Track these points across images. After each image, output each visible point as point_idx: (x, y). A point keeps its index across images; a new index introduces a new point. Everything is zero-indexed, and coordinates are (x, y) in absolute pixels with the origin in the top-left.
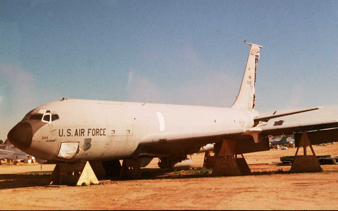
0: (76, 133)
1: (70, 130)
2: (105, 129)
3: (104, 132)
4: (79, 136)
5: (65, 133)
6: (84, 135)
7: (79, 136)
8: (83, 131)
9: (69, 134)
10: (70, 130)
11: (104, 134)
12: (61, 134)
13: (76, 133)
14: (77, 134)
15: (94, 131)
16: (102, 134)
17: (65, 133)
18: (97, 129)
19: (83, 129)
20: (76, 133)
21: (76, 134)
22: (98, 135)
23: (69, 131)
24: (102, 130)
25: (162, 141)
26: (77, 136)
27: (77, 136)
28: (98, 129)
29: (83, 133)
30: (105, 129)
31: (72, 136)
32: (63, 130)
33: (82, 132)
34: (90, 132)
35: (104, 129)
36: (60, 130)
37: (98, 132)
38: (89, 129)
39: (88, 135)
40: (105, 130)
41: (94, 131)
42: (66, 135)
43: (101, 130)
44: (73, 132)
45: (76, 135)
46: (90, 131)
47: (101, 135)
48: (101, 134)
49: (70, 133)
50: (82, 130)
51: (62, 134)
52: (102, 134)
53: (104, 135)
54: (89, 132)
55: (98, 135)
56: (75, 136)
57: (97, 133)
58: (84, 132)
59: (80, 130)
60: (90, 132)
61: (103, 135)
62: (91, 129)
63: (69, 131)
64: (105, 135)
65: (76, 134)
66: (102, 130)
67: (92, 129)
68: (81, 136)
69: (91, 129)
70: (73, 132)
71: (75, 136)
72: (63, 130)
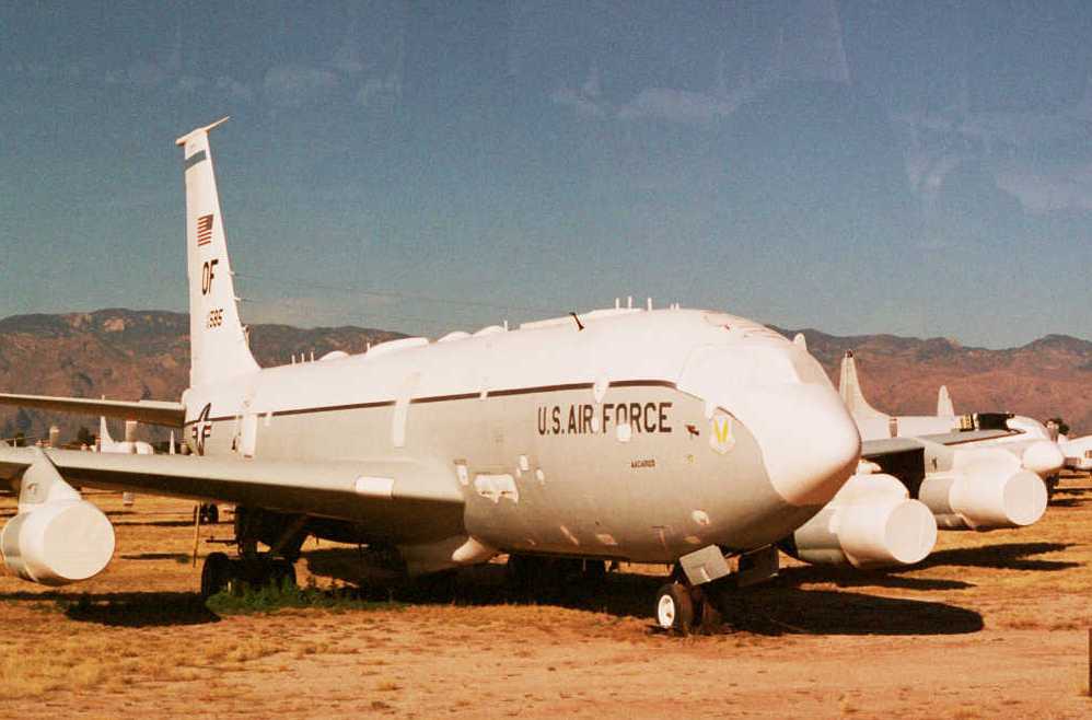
2: (669, 405)
3: (663, 417)
5: (551, 425)
11: (665, 424)
16: (654, 426)
17: (551, 425)
22: (639, 430)
26: (575, 432)
28: (637, 405)
29: (588, 419)
30: (669, 405)
35: (663, 405)
39: (605, 431)
40: (664, 409)
42: (552, 432)
43: (650, 410)
45: (572, 430)
46: (609, 412)
48: (650, 425)
50: (587, 407)
52: (654, 426)
54: (606, 418)
55: (639, 430)
57: (634, 422)
59: (580, 407)
61: (657, 428)
62: (611, 406)
64: (669, 430)
65: (572, 426)
67: (616, 406)
68: (585, 431)
69: (611, 406)
71: (569, 432)
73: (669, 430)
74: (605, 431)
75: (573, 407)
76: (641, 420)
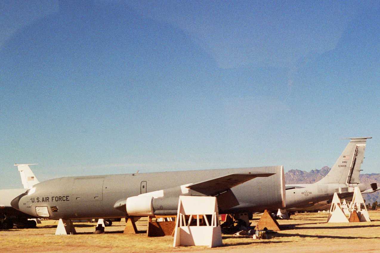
2: (68, 196)
3: (67, 198)
8: (48, 198)
9: (38, 201)
11: (68, 199)
14: (44, 201)
15: (57, 198)
18: (59, 197)
21: (43, 201)
29: (48, 199)
35: (67, 196)
38: (52, 197)
40: (67, 197)
41: (57, 198)
43: (64, 197)
46: (53, 198)
51: (34, 201)
53: (67, 200)
54: (52, 199)
56: (42, 202)
57: (60, 200)
62: (54, 197)
69: (54, 197)
76: (62, 199)
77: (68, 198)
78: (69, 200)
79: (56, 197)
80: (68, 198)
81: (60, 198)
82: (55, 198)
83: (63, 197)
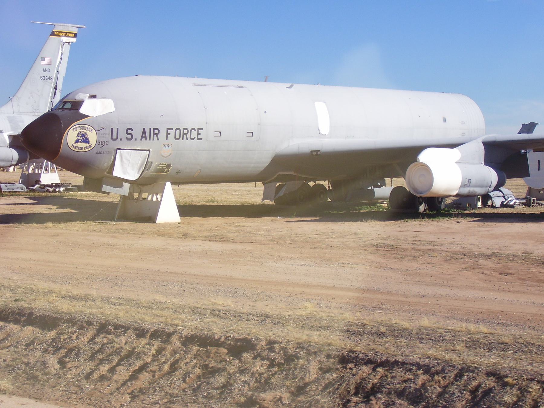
0: (144, 136)
1: (132, 130)
2: (202, 129)
3: (199, 134)
4: (150, 140)
5: (122, 134)
6: (158, 139)
7: (150, 140)
8: (156, 132)
9: (129, 137)
10: (132, 130)
12: (115, 137)
13: (143, 135)
14: (145, 137)
15: (178, 131)
16: (195, 138)
17: (122, 134)
18: (184, 129)
19: (157, 129)
20: (144, 136)
21: (142, 137)
22: (187, 139)
23: (129, 132)
24: (195, 131)
25: (314, 153)
26: (146, 140)
27: (146, 140)
28: (187, 129)
29: (157, 134)
30: (202, 129)
31: (136, 139)
32: (118, 129)
33: (154, 134)
34: (169, 134)
35: (199, 129)
36: (112, 129)
37: (186, 134)
38: (168, 129)
39: (167, 139)
41: (178, 131)
43: (193, 131)
44: (137, 134)
45: (144, 139)
46: (169, 131)
47: (193, 139)
48: (192, 137)
49: (131, 134)
50: (154, 129)
52: (195, 138)
53: (198, 139)
54: (168, 134)
55: (187, 139)
56: (141, 140)
57: (185, 136)
58: (159, 133)
59: (150, 129)
60: (169, 134)
61: (196, 138)
62: (172, 129)
63: (129, 132)
66: (195, 131)
67: (174, 129)
68: (153, 140)
69: (172, 129)
70: (137, 134)
71: (141, 140)
72: (118, 129)
73: (201, 139)
74: (167, 139)
75: (144, 129)
76: (188, 135)
77: (200, 134)
78: (201, 139)
79: (177, 129)
80: (200, 134)
81: (186, 132)
82: (174, 131)
83: (191, 130)
